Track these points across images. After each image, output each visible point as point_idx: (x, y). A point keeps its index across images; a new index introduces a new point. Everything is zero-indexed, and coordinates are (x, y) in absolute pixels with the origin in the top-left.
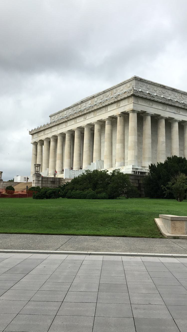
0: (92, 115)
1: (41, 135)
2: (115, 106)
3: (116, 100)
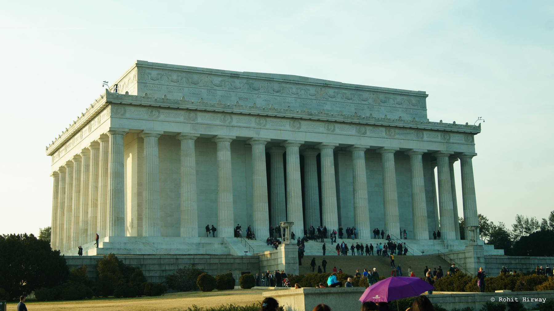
1: (168, 119)
2: (438, 137)
3: (448, 129)
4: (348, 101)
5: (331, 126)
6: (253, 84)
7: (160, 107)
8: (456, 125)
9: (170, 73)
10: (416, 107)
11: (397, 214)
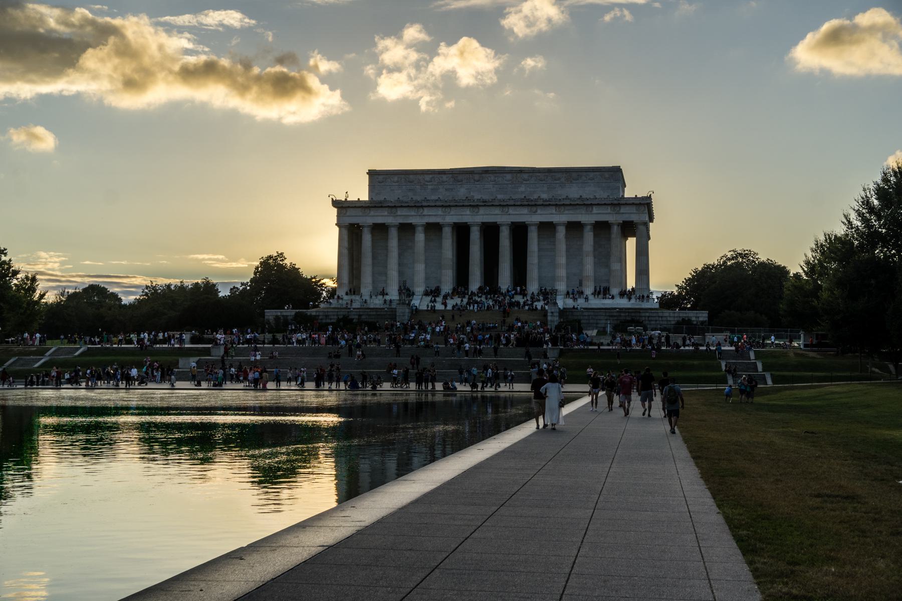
0: (553, 210)
2: (609, 210)
5: (506, 209)
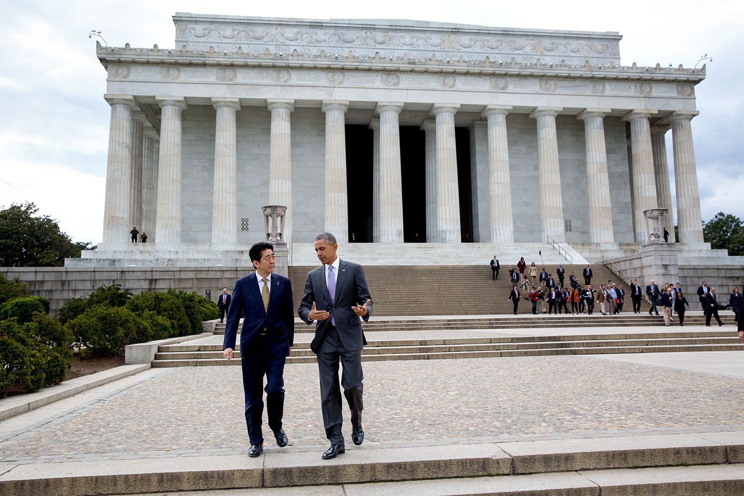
0: (534, 86)
2: (632, 90)
3: (647, 76)
4: (492, 51)
5: (449, 80)
6: (344, 34)
7: (177, 65)
8: (661, 69)
9: (222, 27)
10: (602, 55)
11: (561, 206)
